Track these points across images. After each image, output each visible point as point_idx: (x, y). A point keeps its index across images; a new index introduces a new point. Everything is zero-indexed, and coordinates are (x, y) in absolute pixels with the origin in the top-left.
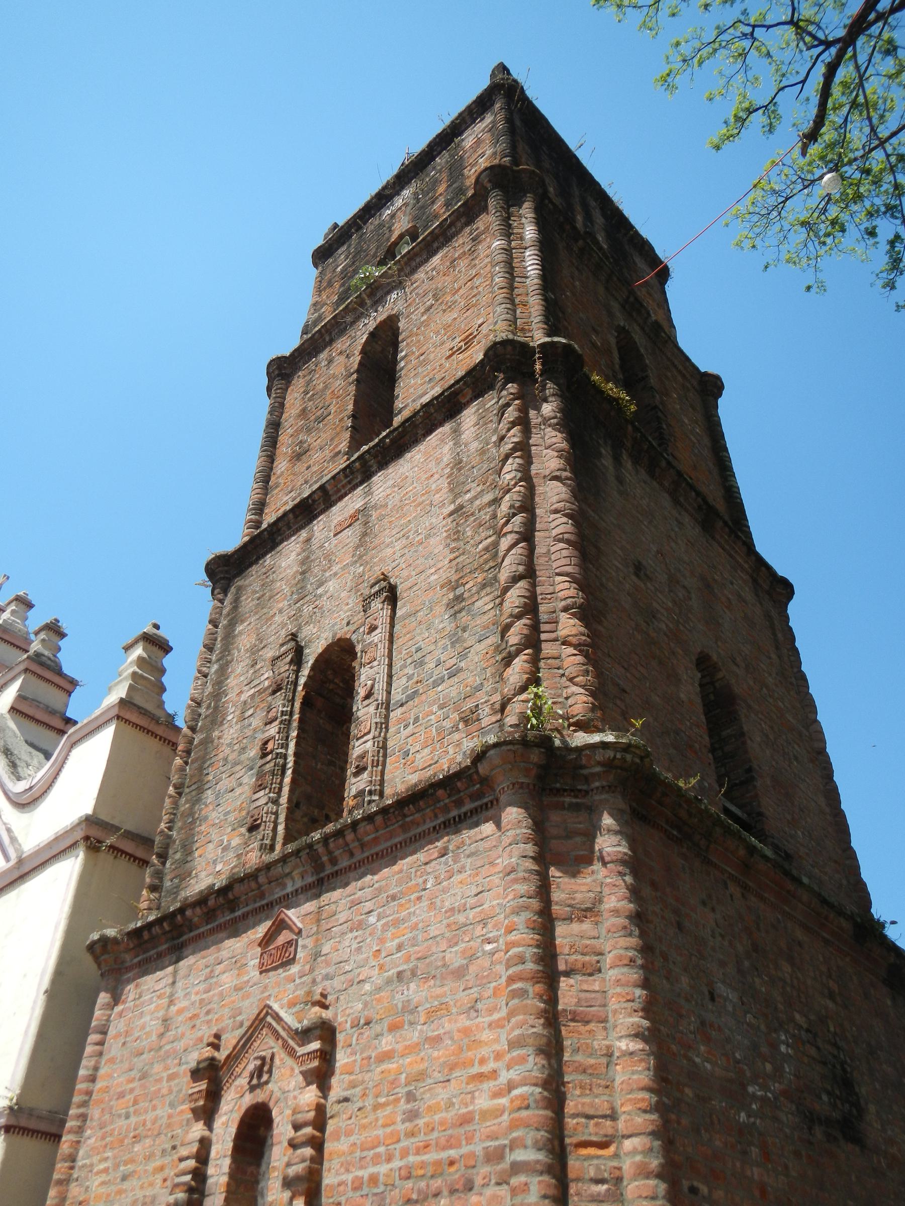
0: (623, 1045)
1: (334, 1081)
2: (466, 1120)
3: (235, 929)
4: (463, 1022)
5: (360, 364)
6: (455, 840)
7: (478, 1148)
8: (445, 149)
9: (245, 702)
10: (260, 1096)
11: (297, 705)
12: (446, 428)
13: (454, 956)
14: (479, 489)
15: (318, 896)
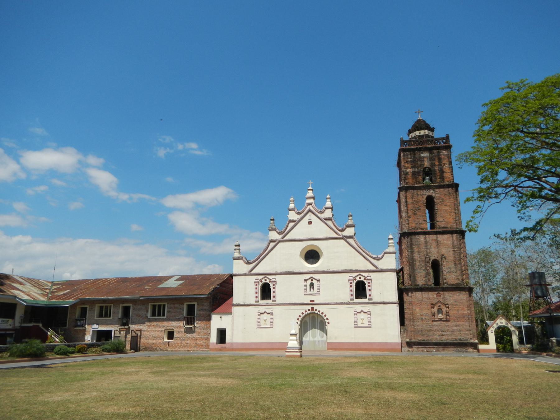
3: (431, 291)
11: (431, 265)
12: (451, 235)
13: (461, 301)
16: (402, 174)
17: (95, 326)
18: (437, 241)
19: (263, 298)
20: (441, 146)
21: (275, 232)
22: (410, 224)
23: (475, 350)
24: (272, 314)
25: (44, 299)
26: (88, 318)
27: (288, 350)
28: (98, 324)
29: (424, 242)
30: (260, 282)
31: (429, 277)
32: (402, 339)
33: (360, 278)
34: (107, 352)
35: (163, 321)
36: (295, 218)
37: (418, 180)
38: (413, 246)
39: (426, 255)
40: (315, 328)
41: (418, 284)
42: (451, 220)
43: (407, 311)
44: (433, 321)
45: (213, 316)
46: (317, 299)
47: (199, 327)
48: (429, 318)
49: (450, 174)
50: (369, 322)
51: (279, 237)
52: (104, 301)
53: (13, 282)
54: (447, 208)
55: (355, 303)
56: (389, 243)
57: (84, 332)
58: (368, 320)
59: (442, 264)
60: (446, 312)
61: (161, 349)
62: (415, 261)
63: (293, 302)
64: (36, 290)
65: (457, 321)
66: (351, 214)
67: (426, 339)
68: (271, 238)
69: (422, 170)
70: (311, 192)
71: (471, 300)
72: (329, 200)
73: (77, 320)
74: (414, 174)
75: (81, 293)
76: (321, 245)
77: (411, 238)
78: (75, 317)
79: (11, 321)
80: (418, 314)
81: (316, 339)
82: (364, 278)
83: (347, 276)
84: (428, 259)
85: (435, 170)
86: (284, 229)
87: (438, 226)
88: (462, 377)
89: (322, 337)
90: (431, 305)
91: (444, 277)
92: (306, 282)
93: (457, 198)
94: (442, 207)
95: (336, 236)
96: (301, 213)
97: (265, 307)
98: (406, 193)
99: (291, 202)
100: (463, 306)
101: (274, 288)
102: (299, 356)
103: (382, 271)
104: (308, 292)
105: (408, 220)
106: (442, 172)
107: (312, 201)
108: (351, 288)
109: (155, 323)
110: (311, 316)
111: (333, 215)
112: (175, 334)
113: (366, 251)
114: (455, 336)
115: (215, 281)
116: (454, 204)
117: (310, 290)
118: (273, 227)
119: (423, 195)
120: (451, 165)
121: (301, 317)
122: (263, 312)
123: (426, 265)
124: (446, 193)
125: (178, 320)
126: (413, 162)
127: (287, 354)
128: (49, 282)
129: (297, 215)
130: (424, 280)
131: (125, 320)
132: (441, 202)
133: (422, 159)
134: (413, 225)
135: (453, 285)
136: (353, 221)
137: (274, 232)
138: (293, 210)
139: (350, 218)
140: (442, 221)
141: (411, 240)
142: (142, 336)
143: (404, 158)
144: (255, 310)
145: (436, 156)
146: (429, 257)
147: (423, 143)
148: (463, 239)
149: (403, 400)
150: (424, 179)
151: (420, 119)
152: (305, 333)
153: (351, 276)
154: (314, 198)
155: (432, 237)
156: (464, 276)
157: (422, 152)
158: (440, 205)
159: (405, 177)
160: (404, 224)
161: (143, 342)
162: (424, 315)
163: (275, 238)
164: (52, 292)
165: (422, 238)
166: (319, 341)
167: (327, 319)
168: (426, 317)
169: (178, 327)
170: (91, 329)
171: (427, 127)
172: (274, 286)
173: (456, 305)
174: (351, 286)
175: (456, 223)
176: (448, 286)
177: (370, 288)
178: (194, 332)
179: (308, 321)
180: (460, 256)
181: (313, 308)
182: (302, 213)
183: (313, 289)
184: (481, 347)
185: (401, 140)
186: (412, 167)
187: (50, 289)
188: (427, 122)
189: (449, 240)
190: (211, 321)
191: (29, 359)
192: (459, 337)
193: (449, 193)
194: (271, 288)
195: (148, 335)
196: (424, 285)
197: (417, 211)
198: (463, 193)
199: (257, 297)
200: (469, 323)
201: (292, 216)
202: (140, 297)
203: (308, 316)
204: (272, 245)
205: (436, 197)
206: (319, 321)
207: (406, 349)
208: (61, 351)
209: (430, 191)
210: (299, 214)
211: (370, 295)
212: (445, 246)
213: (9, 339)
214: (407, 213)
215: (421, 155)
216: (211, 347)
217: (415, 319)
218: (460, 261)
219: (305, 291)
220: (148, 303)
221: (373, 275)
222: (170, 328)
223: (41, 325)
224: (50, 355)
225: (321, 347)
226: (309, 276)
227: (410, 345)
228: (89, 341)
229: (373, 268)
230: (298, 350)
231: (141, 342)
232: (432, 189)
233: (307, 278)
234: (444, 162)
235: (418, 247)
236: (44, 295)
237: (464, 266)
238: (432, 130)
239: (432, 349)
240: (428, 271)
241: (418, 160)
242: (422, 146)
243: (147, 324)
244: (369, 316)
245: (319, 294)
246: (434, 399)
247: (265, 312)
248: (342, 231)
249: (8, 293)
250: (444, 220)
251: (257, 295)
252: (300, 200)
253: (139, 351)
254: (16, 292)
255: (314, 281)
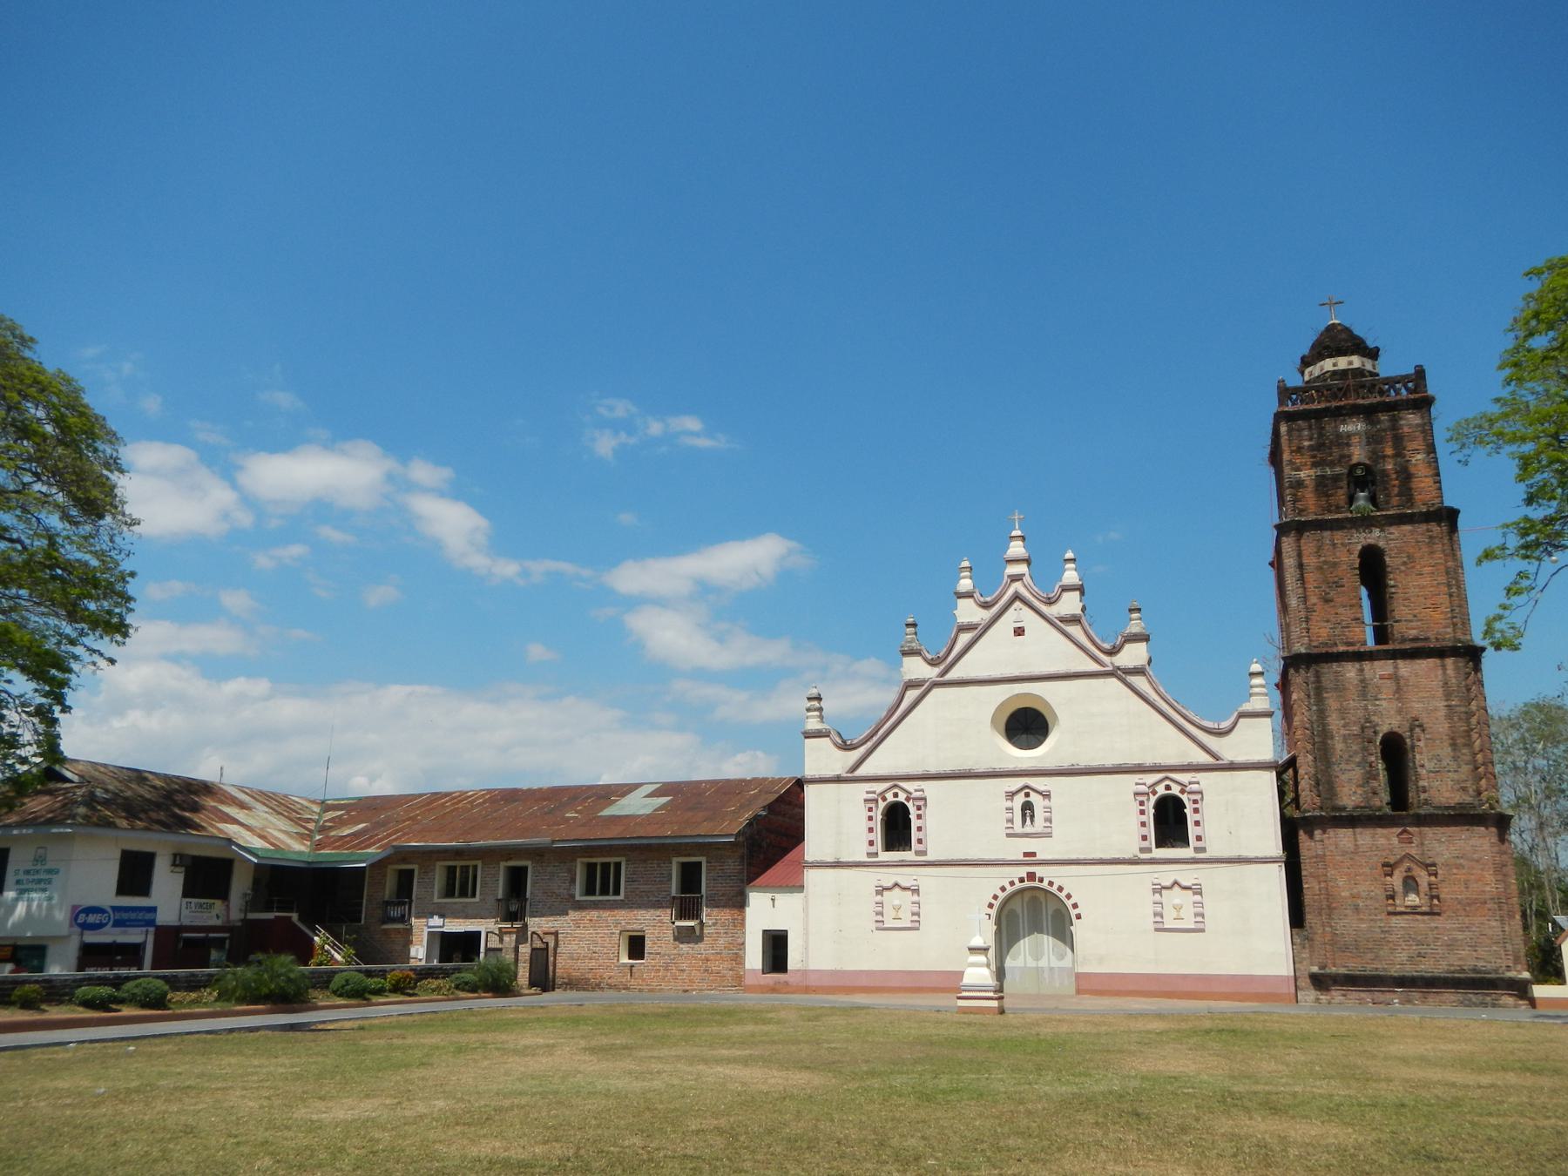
0: (1514, 881)
1: (1439, 876)
2: (1484, 891)
4: (1480, 872)
5: (1361, 564)
6: (1471, 828)
7: (1487, 897)
8: (1387, 411)
9: (1344, 735)
10: (1410, 874)
11: (1379, 751)
12: (1438, 661)
13: (1475, 856)
14: (1458, 703)
15: (1418, 827)
16: (1287, 485)
17: (436, 921)
18: (1395, 677)
19: (890, 845)
20: (1403, 400)
21: (919, 658)
22: (1314, 630)
23: (1521, 1002)
24: (916, 891)
25: (302, 848)
26: (417, 899)
27: (964, 994)
28: (442, 916)
29: (1356, 682)
30: (880, 801)
31: (1374, 784)
32: (1297, 966)
33: (1168, 787)
34: (469, 991)
35: (617, 908)
36: (975, 620)
37: (1332, 500)
38: (1325, 695)
39: (1363, 721)
40: (1041, 931)
41: (1341, 804)
42: (1437, 616)
43: (1310, 886)
44: (1390, 914)
45: (750, 894)
46: (1044, 850)
47: (714, 924)
48: (1377, 905)
49: (1430, 481)
50: (1196, 915)
51: (931, 673)
52: (458, 853)
53: (222, 802)
54: (1425, 581)
55: (1154, 859)
56: (1252, 687)
57: (407, 937)
58: (1192, 911)
59: (1413, 747)
60: (1430, 889)
61: (610, 987)
62: (1332, 738)
63: (975, 858)
64: (283, 824)
65: (1464, 913)
66: (1136, 604)
67: (1369, 967)
68: (907, 677)
69: (1345, 471)
70: (1021, 543)
71: (1505, 853)
72: (1073, 565)
73: (387, 903)
74: (1323, 485)
75: (397, 831)
76: (1051, 695)
77: (1317, 671)
78: (384, 896)
79: (218, 903)
80: (1343, 894)
81: (1043, 963)
82: (1179, 788)
83: (1129, 782)
84: (1369, 732)
85: (1384, 470)
86: (945, 650)
87: (1397, 635)
88: (1486, 1080)
89: (1062, 957)
90: (1383, 866)
91: (1421, 783)
92: (1012, 801)
93: (1453, 550)
94: (1409, 579)
95: (1093, 667)
96: (993, 605)
97: (896, 870)
98: (1298, 540)
99: (962, 574)
100: (1482, 870)
101: (919, 817)
102: (997, 1011)
103: (1232, 767)
104: (1018, 828)
105: (1307, 620)
106: (1406, 475)
107: (1021, 569)
108: (1143, 818)
109: (594, 914)
110: (1027, 895)
111: (1084, 609)
112: (648, 943)
113: (1184, 711)
114: (1460, 959)
115: (755, 797)
116: (1447, 568)
117: (1024, 822)
118: (914, 644)
119: (1350, 543)
120: (1432, 455)
121: (1000, 900)
122: (889, 884)
123: (1365, 749)
124: (1420, 538)
125: (657, 905)
126: (1319, 451)
127: (961, 1003)
128: (313, 802)
129: (981, 610)
130: (1359, 792)
131: (514, 906)
132: (1404, 563)
133: (1344, 441)
134: (1323, 633)
135: (1448, 808)
136: (1143, 624)
137: (917, 660)
138: (969, 595)
139: (1135, 615)
140: (1411, 621)
141: (1318, 675)
142: (559, 950)
143: (1289, 440)
144: (869, 879)
145: (1384, 430)
146: (1374, 726)
147: (1345, 392)
148: (1476, 673)
149: (1308, 1145)
150: (1351, 499)
151: (1333, 324)
152: (1010, 946)
153: (1141, 781)
154: (1028, 561)
155: (1383, 668)
156: (1483, 782)
157: (1345, 420)
158: (1401, 572)
159: (1295, 495)
160: (1296, 631)
161: (564, 964)
162: (1363, 893)
163: (921, 676)
164: (322, 829)
165: (1350, 671)
166: (1051, 969)
167: (1075, 906)
168: (1369, 902)
169: (657, 924)
170: (425, 928)
171: (1356, 346)
172: (919, 812)
173: (1463, 867)
174: (1142, 812)
175: (1455, 625)
176: (1432, 811)
177: (1197, 817)
178: (700, 939)
179: (1019, 911)
180: (1468, 720)
181: (1034, 873)
182: (996, 603)
183: (1032, 821)
184: (1540, 991)
185: (1278, 387)
186: (1314, 465)
187: (317, 822)
188: (1358, 331)
189: (1433, 676)
190: (747, 909)
191: (269, 1006)
192: (1469, 963)
193: (1431, 537)
194: (913, 817)
195: (576, 947)
196: (1362, 807)
197: (1332, 593)
198: (1473, 537)
199: (871, 843)
200: (1502, 921)
201: (968, 612)
202: (553, 842)
203: (1019, 897)
204: (912, 695)
205: (1391, 550)
206: (1050, 912)
207: (1309, 995)
208: (349, 987)
209: (1371, 532)
210: (986, 606)
211: (1199, 838)
212: (1420, 694)
213: (214, 955)
214: (1305, 599)
215: (1342, 428)
216: (749, 981)
217: (1335, 908)
218: (1469, 736)
219: (1010, 825)
220: (574, 860)
221: (1206, 780)
222: (635, 927)
223: (295, 916)
224: (320, 998)
225: (1057, 985)
226: (1017, 783)
227: (1321, 982)
228: (420, 960)
229: (1204, 758)
230: (991, 994)
231: (559, 965)
232: (1377, 527)
233: (1014, 789)
234: (1411, 446)
235: (1338, 696)
236: (301, 837)
237: (1481, 751)
238: (1373, 354)
239: (1388, 996)
240: (1371, 766)
241: (1331, 442)
242: (1342, 403)
243: (573, 915)
244: (1198, 898)
245: (1049, 835)
246: (1403, 1143)
247: (896, 885)
248: (1112, 652)
249: (212, 832)
250: (1415, 616)
251: (872, 836)
252: (989, 567)
253: (553, 990)
254: (231, 829)
255: (1034, 798)
